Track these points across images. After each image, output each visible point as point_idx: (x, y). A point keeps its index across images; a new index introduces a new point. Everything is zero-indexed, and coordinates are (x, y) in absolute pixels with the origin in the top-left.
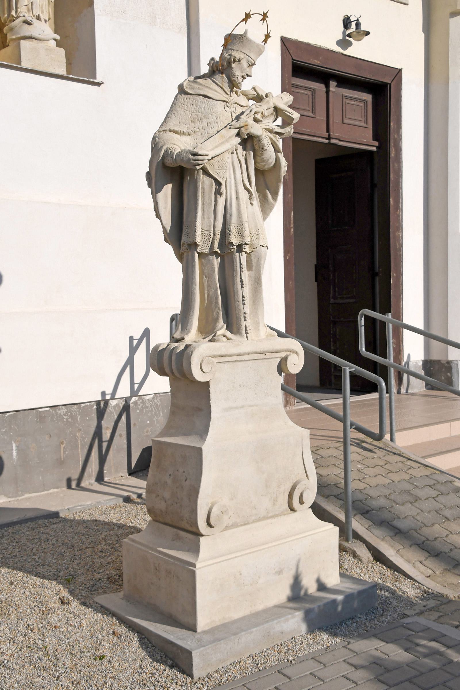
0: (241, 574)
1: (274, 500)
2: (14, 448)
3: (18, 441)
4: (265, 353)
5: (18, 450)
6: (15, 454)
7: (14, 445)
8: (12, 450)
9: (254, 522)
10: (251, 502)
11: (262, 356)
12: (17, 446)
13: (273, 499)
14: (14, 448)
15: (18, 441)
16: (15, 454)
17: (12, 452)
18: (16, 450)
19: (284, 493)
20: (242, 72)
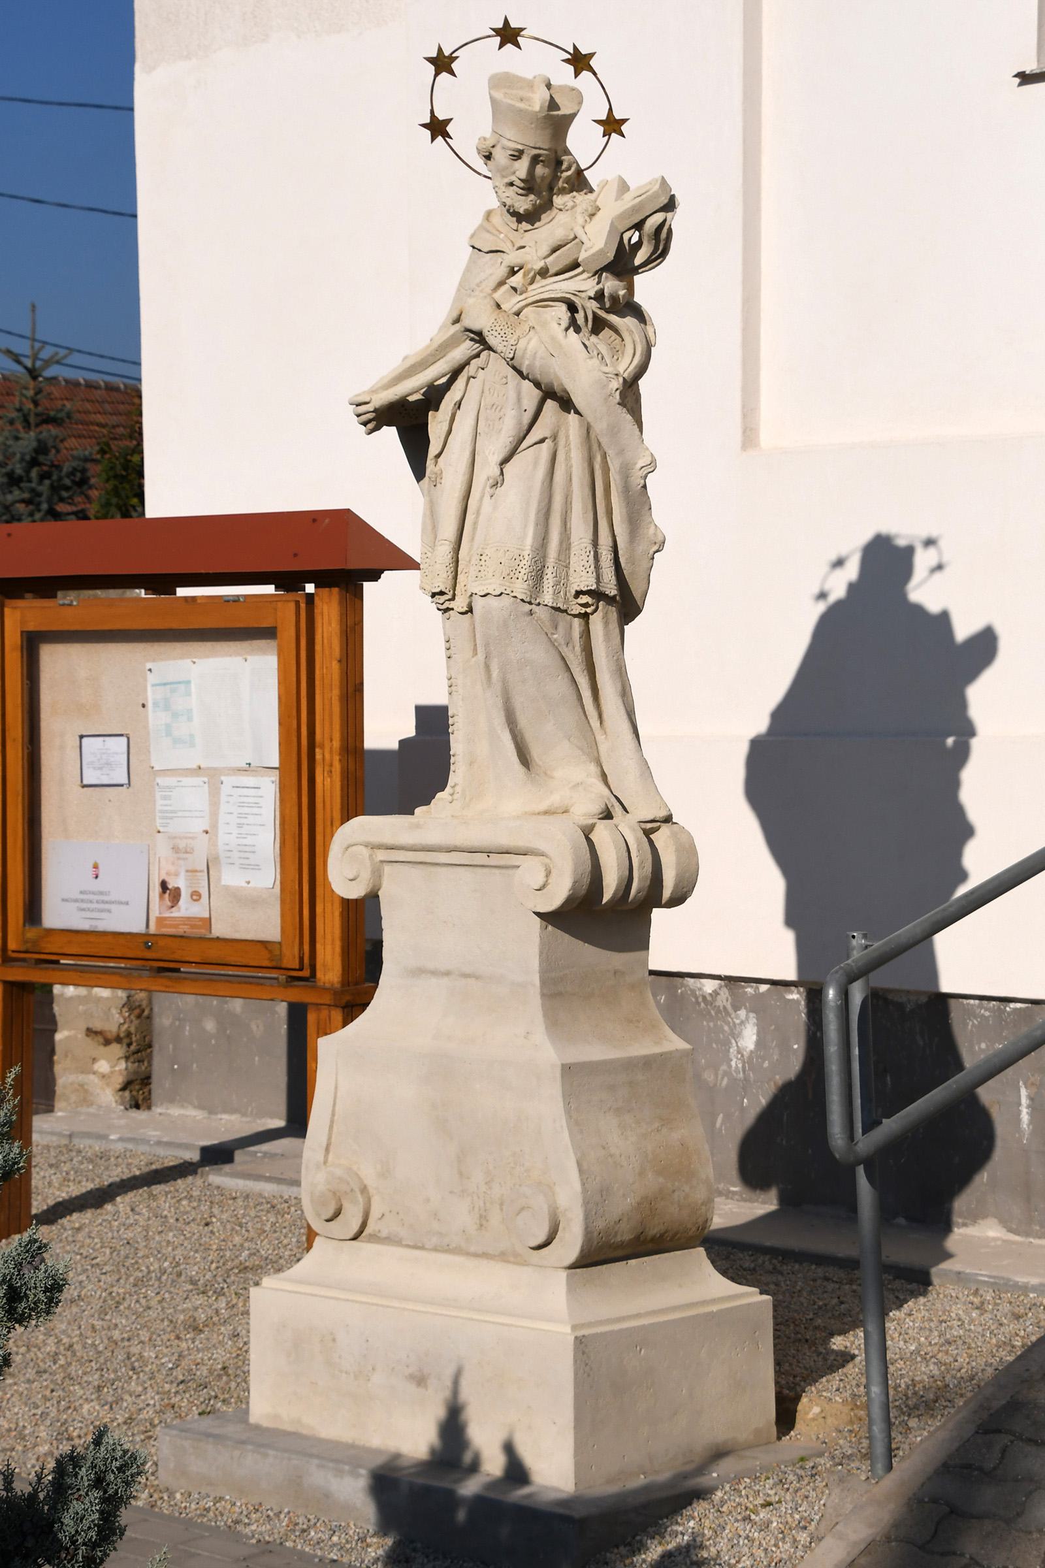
0: (334, 1340)
1: (481, 1216)
2: (1024, 1101)
3: (1033, 1084)
4: (489, 852)
5: (1033, 1107)
6: (1025, 1116)
7: (1024, 1092)
8: (1020, 1104)
9: (435, 1249)
10: (428, 1200)
11: (480, 858)
12: (1031, 1098)
13: (476, 1210)
14: (1024, 1101)
15: (1033, 1084)
16: (1025, 1116)
17: (1019, 1112)
18: (1028, 1107)
19: (501, 1204)
20: (503, 177)
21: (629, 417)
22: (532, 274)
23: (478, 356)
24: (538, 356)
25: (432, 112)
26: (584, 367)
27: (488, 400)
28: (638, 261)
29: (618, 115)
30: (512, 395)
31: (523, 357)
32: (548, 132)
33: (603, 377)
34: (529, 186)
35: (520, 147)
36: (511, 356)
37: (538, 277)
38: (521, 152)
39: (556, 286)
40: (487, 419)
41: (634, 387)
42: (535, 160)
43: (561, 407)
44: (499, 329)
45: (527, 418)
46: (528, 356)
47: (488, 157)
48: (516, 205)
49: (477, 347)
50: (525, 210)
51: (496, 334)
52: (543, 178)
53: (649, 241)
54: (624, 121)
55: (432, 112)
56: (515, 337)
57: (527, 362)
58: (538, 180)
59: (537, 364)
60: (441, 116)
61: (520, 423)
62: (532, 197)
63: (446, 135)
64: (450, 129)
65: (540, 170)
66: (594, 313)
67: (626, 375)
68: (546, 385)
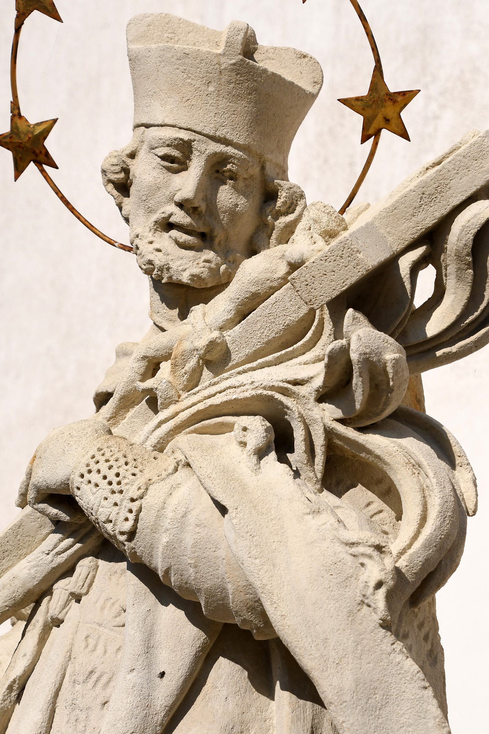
20: (150, 211)
21: (411, 666)
22: (192, 363)
23: (68, 570)
24: (192, 519)
25: (15, 106)
26: (302, 554)
27: (83, 661)
28: (434, 326)
29: (394, 83)
30: (133, 635)
31: (155, 529)
32: (243, 106)
33: (343, 553)
34: (201, 226)
35: (185, 136)
36: (127, 526)
37: (206, 373)
38: (186, 148)
39: (242, 378)
40: (73, 706)
41: (424, 604)
42: (217, 171)
43: (251, 678)
44: (104, 467)
45: (165, 693)
46: (166, 523)
47: (123, 187)
48: (174, 266)
49: (68, 546)
50: (193, 277)
51: (95, 477)
52: (233, 213)
53: (459, 279)
54: (407, 96)
55: (15, 106)
56: (141, 480)
57: (164, 539)
58: (224, 218)
59: (189, 539)
60: (33, 115)
61: (147, 705)
62: (210, 255)
63: (44, 159)
64: (51, 144)
65: (226, 196)
66: (329, 433)
67: (402, 563)
68: (210, 594)
